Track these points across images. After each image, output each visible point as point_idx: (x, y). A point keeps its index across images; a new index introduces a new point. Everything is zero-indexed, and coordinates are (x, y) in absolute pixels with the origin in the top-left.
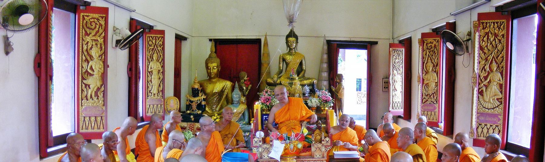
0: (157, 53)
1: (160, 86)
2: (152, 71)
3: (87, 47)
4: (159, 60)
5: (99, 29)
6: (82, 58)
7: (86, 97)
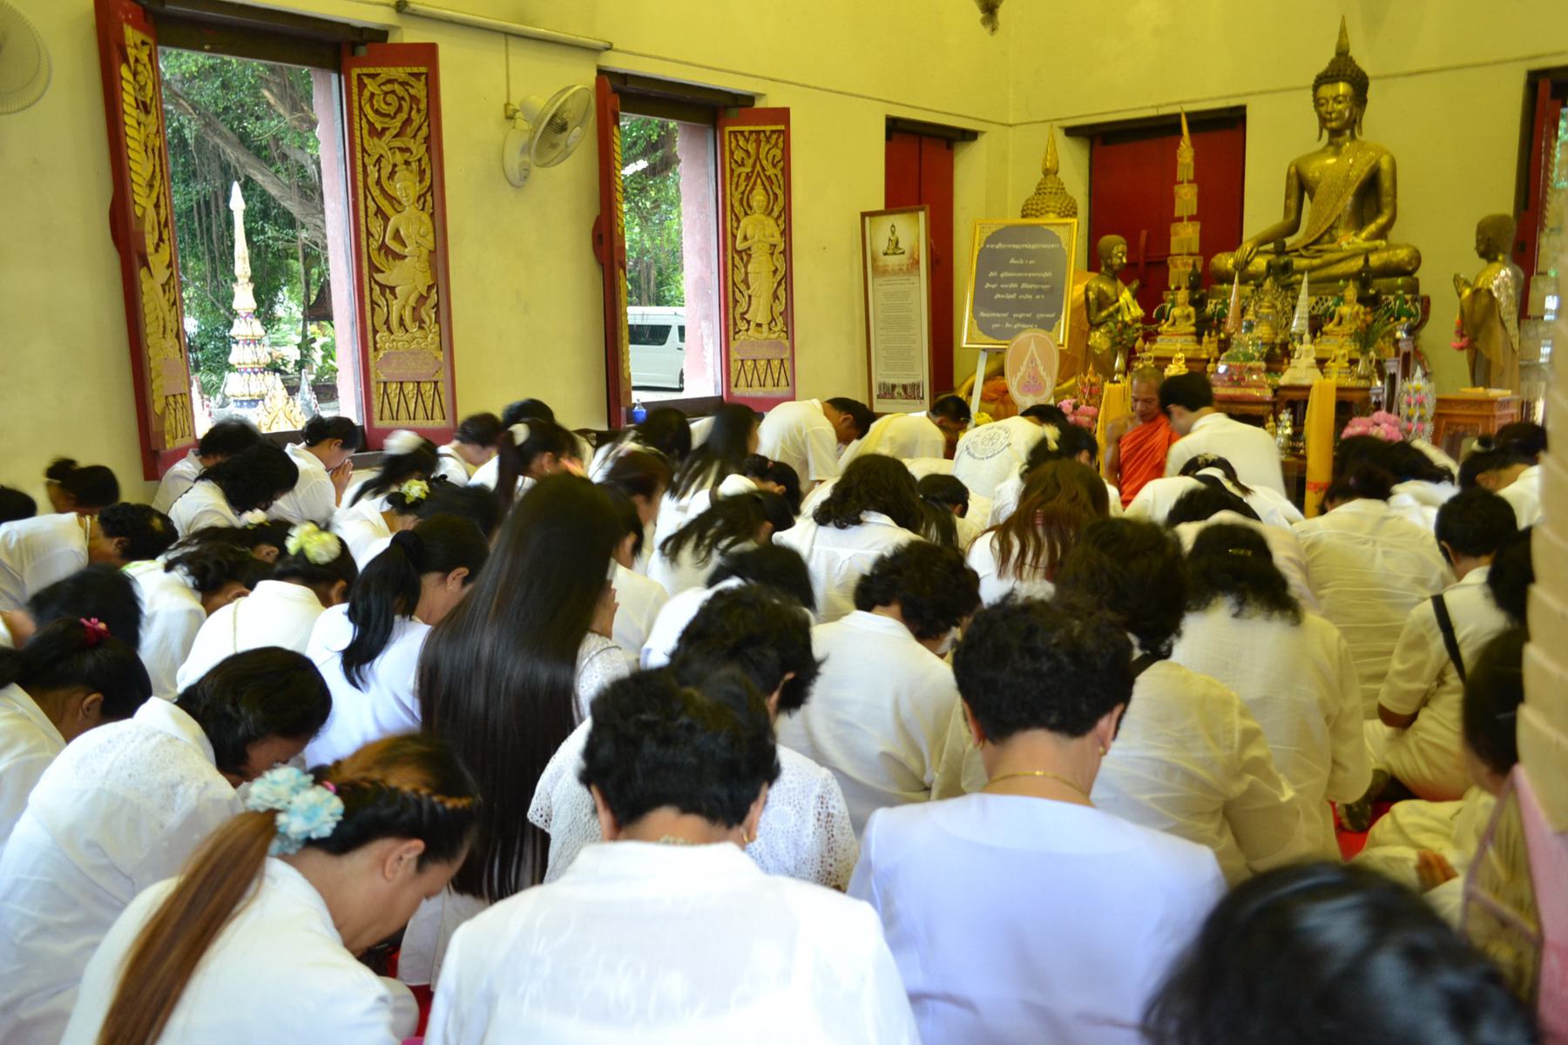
0: (765, 189)
1: (776, 297)
2: (749, 249)
3: (379, 171)
4: (772, 209)
5: (409, 114)
6: (366, 207)
7: (387, 322)
